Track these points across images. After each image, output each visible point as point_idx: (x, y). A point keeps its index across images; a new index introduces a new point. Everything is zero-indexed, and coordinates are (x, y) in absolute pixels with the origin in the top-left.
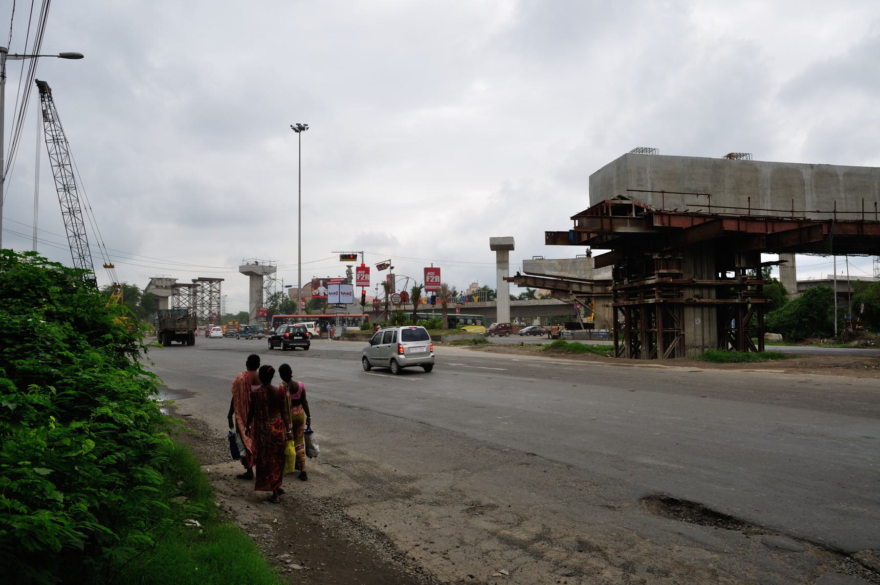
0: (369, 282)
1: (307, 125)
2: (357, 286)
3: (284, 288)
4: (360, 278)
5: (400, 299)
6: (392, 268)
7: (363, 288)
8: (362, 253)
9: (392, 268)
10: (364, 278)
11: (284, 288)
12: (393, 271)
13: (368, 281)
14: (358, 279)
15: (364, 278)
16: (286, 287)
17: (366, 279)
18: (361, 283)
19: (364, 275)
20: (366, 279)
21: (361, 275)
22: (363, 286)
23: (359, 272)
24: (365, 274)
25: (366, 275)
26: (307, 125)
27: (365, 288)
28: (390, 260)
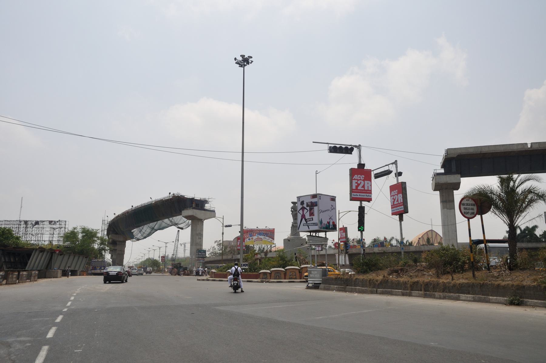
0: (371, 193)
1: (251, 57)
2: (352, 199)
3: (224, 227)
4: (357, 187)
5: (475, 208)
6: (400, 174)
7: (361, 203)
8: (359, 147)
9: (400, 174)
10: (363, 186)
11: (224, 227)
12: (401, 179)
13: (370, 192)
14: (354, 187)
15: (363, 186)
16: (227, 226)
17: (366, 188)
18: (358, 195)
19: (363, 182)
20: (366, 188)
21: (359, 182)
22: (361, 200)
23: (356, 177)
24: (364, 180)
25: (366, 182)
26: (251, 57)
27: (364, 204)
28: (395, 163)
